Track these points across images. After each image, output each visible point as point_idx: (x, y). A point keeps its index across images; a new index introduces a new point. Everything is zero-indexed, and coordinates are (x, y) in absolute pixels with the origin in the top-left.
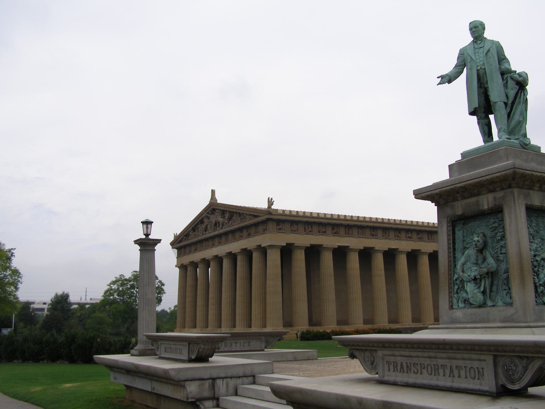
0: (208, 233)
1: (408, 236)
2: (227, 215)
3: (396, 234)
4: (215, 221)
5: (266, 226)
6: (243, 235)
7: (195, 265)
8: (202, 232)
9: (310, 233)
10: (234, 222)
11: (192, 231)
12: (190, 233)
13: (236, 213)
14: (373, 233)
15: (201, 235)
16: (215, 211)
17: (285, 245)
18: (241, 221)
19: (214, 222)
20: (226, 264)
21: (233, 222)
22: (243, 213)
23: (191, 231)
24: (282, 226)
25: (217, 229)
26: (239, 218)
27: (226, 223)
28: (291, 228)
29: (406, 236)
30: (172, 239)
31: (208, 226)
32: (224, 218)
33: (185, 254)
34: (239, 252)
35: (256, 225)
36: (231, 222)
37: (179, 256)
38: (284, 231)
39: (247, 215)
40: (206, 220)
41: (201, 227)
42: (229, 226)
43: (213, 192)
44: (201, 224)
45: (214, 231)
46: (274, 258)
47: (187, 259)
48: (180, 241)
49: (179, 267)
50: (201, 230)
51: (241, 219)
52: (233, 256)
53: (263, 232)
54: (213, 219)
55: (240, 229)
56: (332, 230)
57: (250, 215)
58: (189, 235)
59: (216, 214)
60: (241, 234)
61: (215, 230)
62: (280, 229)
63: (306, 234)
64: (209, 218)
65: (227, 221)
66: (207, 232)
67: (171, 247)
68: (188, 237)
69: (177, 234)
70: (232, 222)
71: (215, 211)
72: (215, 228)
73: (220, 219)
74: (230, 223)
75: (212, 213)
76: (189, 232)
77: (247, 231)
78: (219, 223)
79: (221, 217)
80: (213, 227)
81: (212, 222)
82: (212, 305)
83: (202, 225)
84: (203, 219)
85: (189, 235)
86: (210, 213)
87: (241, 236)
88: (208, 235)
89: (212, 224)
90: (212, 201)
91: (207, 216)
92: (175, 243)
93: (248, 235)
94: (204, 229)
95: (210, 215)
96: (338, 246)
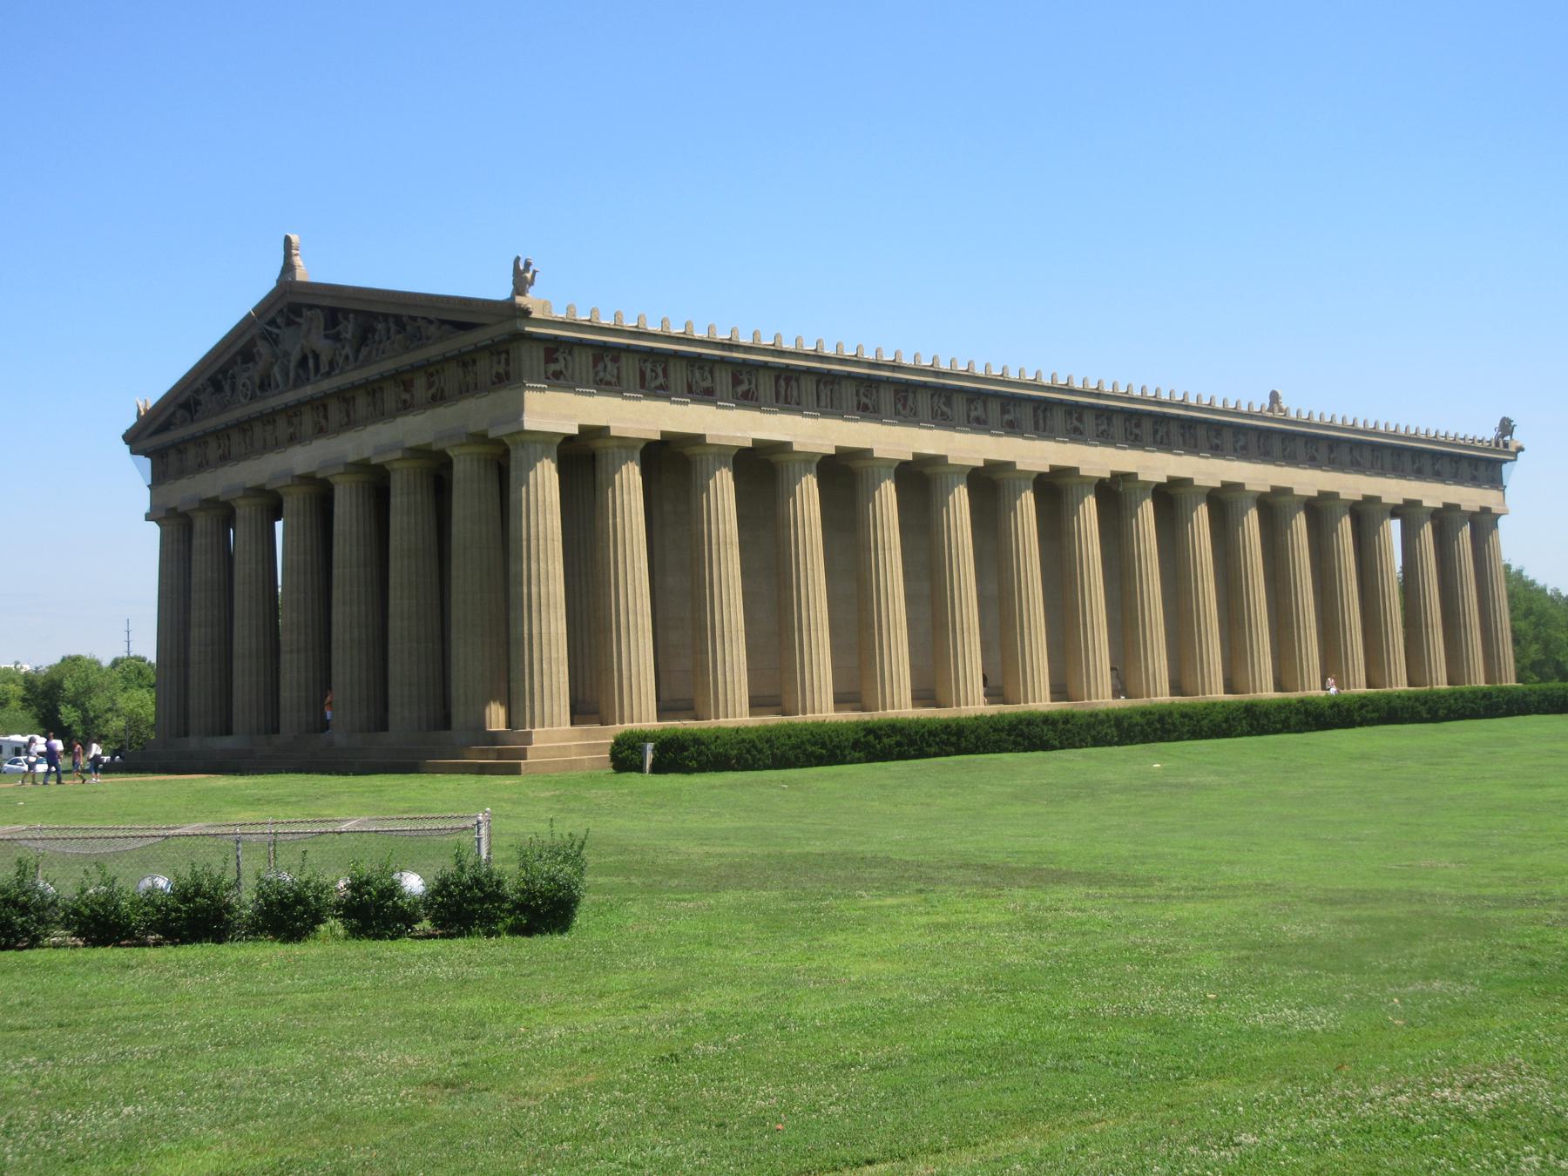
1: (973, 414)
2: (349, 329)
3: (935, 408)
5: (507, 363)
6: (413, 396)
7: (224, 513)
8: (249, 393)
10: (378, 350)
11: (210, 389)
12: (201, 397)
14: (864, 400)
16: (300, 315)
21: (374, 352)
22: (414, 319)
23: (205, 389)
24: (566, 366)
26: (400, 337)
28: (596, 373)
29: (968, 416)
32: (337, 338)
35: (465, 360)
36: (364, 351)
37: (158, 480)
39: (431, 322)
40: (263, 348)
41: (246, 374)
44: (245, 362)
45: (296, 386)
48: (165, 427)
49: (158, 521)
50: (244, 385)
54: (294, 343)
55: (402, 378)
56: (734, 386)
57: (443, 322)
58: (198, 403)
61: (299, 382)
67: (127, 448)
68: (196, 411)
71: (300, 315)
73: (323, 345)
74: (361, 357)
75: (290, 323)
76: (197, 391)
78: (316, 357)
79: (327, 337)
80: (292, 374)
83: (251, 365)
84: (252, 343)
85: (198, 403)
86: (279, 320)
88: (274, 402)
89: (289, 361)
91: (270, 333)
94: (257, 381)
95: (279, 328)
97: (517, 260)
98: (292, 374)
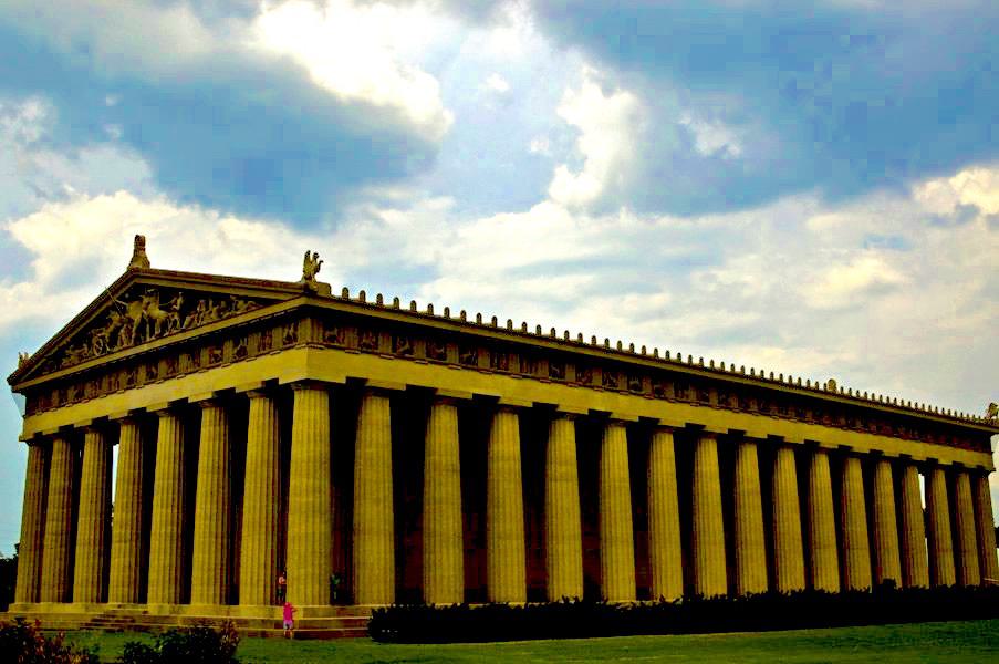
0: (120, 351)
4: (142, 319)
5: (296, 329)
6: (222, 354)
9: (407, 355)
10: (198, 318)
13: (206, 295)
15: (97, 355)
17: (344, 382)
18: (220, 316)
19: (137, 319)
20: (166, 433)
25: (145, 339)
26: (215, 309)
27: (175, 321)
30: (14, 367)
31: (122, 331)
32: (167, 309)
33: (47, 407)
34: (208, 400)
35: (264, 327)
36: (188, 319)
37: (30, 412)
38: (343, 346)
40: (116, 317)
42: (183, 331)
43: (140, 242)
45: (136, 345)
46: (310, 415)
47: (51, 421)
49: (29, 442)
50: (98, 343)
51: (219, 311)
52: (185, 413)
53: (285, 344)
54: (135, 312)
55: (215, 340)
57: (246, 299)
59: (146, 300)
60: (218, 352)
61: (138, 342)
62: (332, 339)
63: (396, 357)
64: (124, 311)
65: (176, 317)
66: (116, 349)
67: (10, 387)
69: (26, 354)
70: (193, 319)
72: (142, 338)
73: (158, 313)
74: (186, 323)
77: (236, 345)
79: (161, 308)
81: (131, 321)
82: (120, 541)
84: (106, 312)
87: (216, 356)
90: (138, 265)
92: (20, 377)
93: (239, 353)
96: (474, 395)
97: (308, 253)
98: (133, 336)
